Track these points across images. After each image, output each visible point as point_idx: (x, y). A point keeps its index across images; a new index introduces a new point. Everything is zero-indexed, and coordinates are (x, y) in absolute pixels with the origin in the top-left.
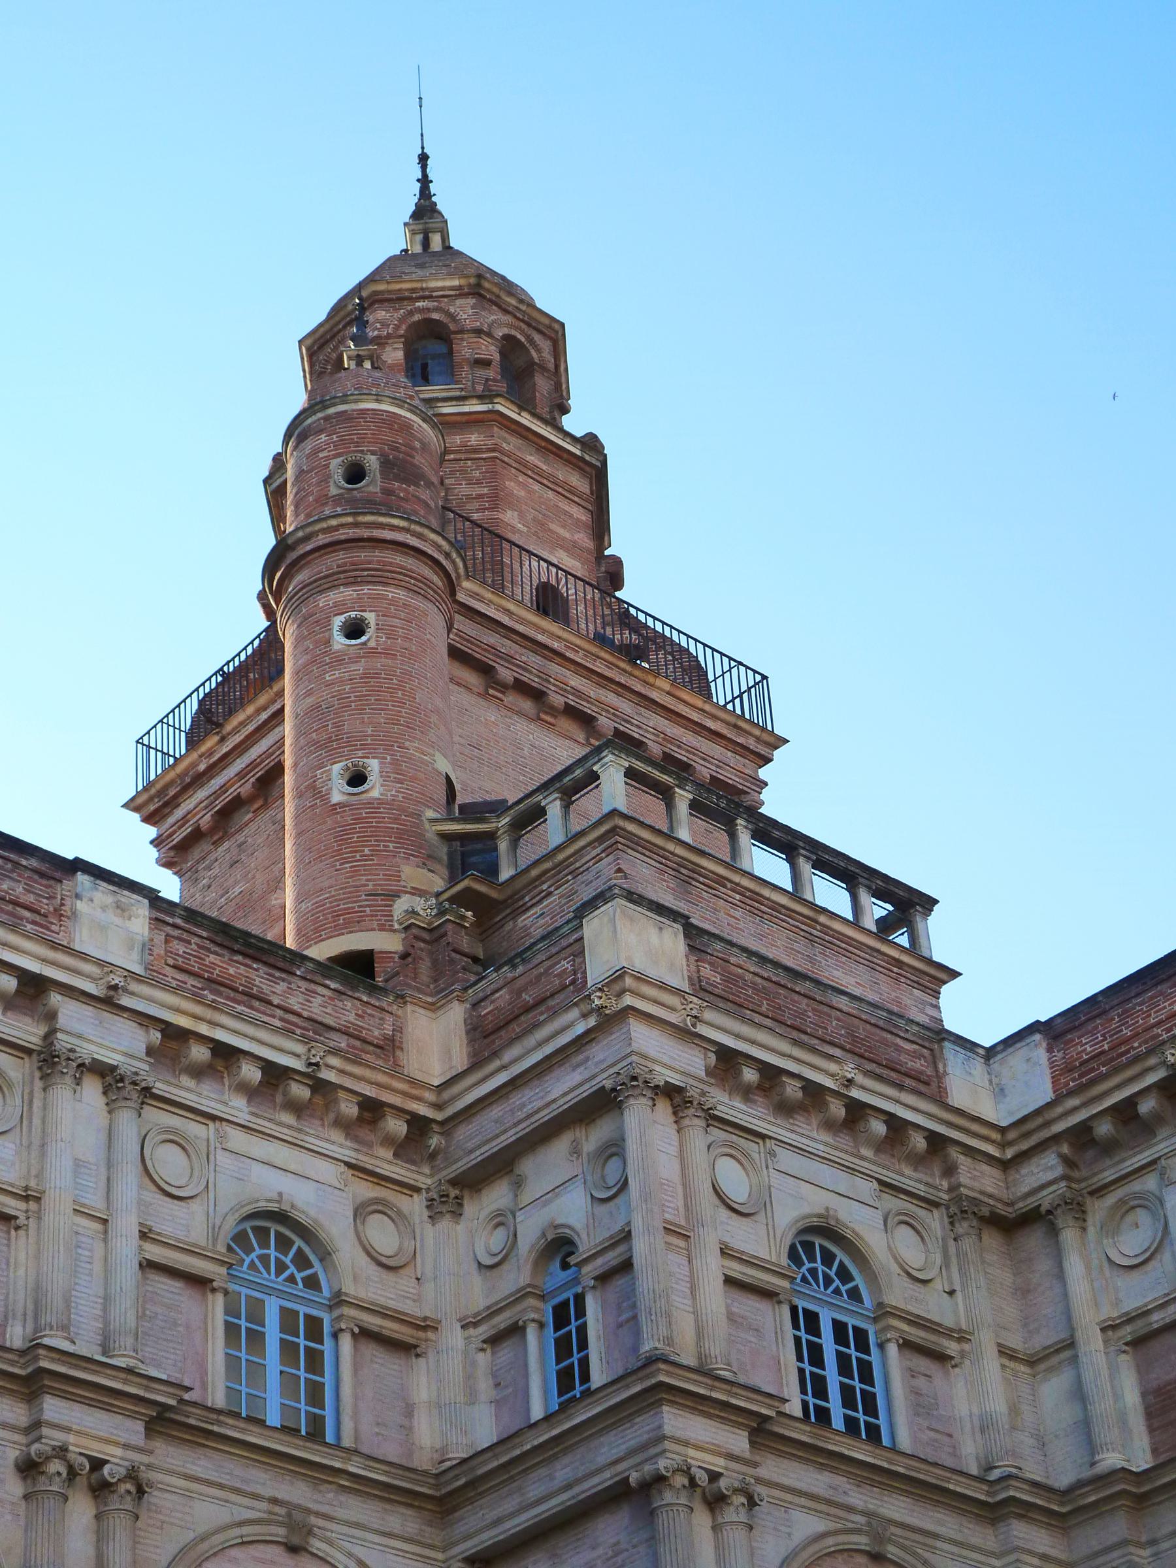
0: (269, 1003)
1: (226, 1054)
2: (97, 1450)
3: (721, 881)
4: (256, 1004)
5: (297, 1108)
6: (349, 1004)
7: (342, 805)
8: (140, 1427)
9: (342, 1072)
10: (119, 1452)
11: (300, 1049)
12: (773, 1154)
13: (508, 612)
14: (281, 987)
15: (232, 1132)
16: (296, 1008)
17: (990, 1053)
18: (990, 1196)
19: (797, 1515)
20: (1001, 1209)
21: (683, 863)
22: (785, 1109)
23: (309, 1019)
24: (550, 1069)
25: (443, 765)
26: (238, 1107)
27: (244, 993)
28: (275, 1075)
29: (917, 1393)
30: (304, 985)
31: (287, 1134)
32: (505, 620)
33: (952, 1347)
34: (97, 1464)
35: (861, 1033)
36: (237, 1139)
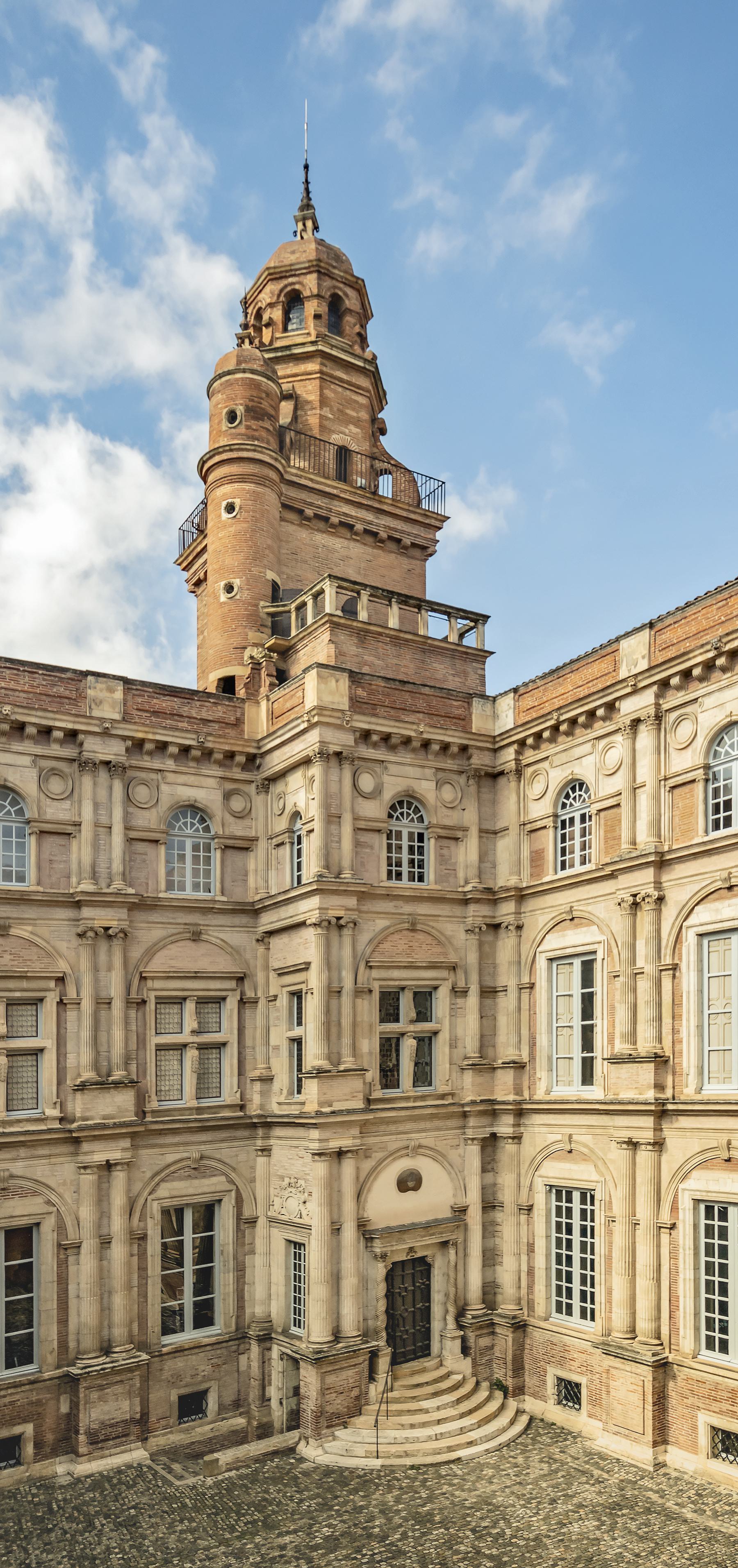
0: (182, 716)
1: (162, 746)
2: (106, 924)
3: (380, 634)
4: (176, 718)
5: (196, 760)
6: (219, 707)
7: (224, 603)
8: (125, 910)
9: (214, 742)
10: (116, 923)
11: (194, 736)
12: (386, 768)
13: (311, 480)
14: (186, 709)
15: (168, 774)
16: (195, 715)
17: (494, 699)
18: (486, 766)
19: (377, 921)
20: (490, 770)
21: (361, 630)
22: (393, 748)
23: (201, 719)
24: (294, 740)
25: (271, 575)
26: (170, 764)
27: (170, 714)
28: (185, 750)
29: (442, 856)
30: (198, 703)
31: (192, 771)
32: (310, 484)
33: (459, 834)
34: (107, 929)
35: (434, 703)
36: (171, 777)
